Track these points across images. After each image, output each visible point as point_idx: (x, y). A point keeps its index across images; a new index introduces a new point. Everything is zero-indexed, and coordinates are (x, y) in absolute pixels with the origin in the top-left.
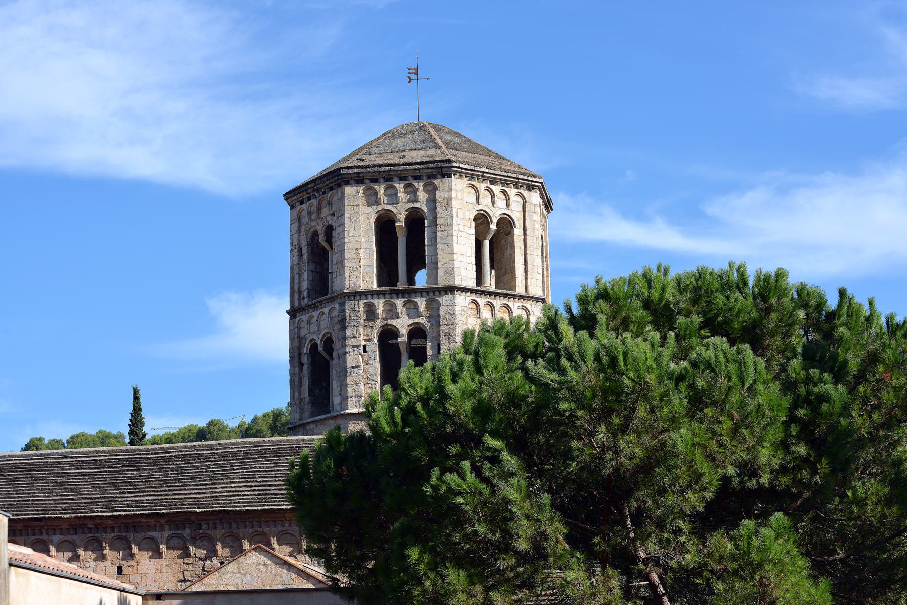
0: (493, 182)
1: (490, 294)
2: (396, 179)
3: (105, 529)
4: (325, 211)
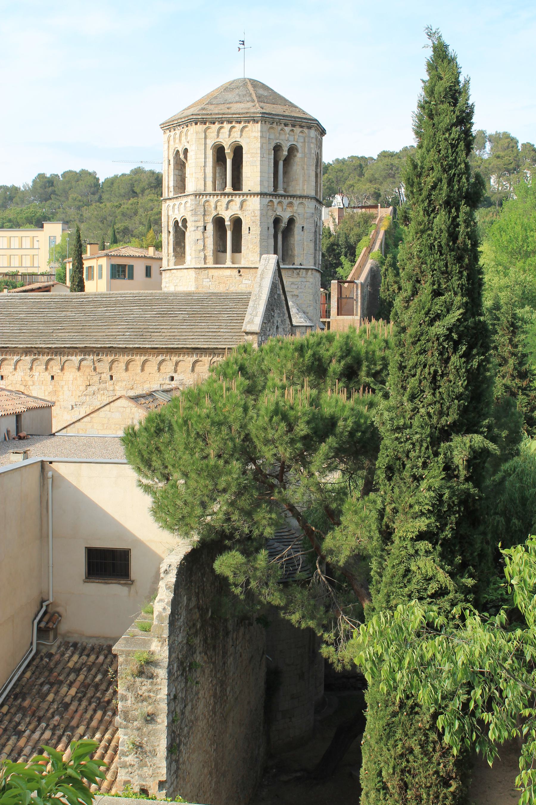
0: (286, 125)
1: (282, 196)
4: (183, 138)
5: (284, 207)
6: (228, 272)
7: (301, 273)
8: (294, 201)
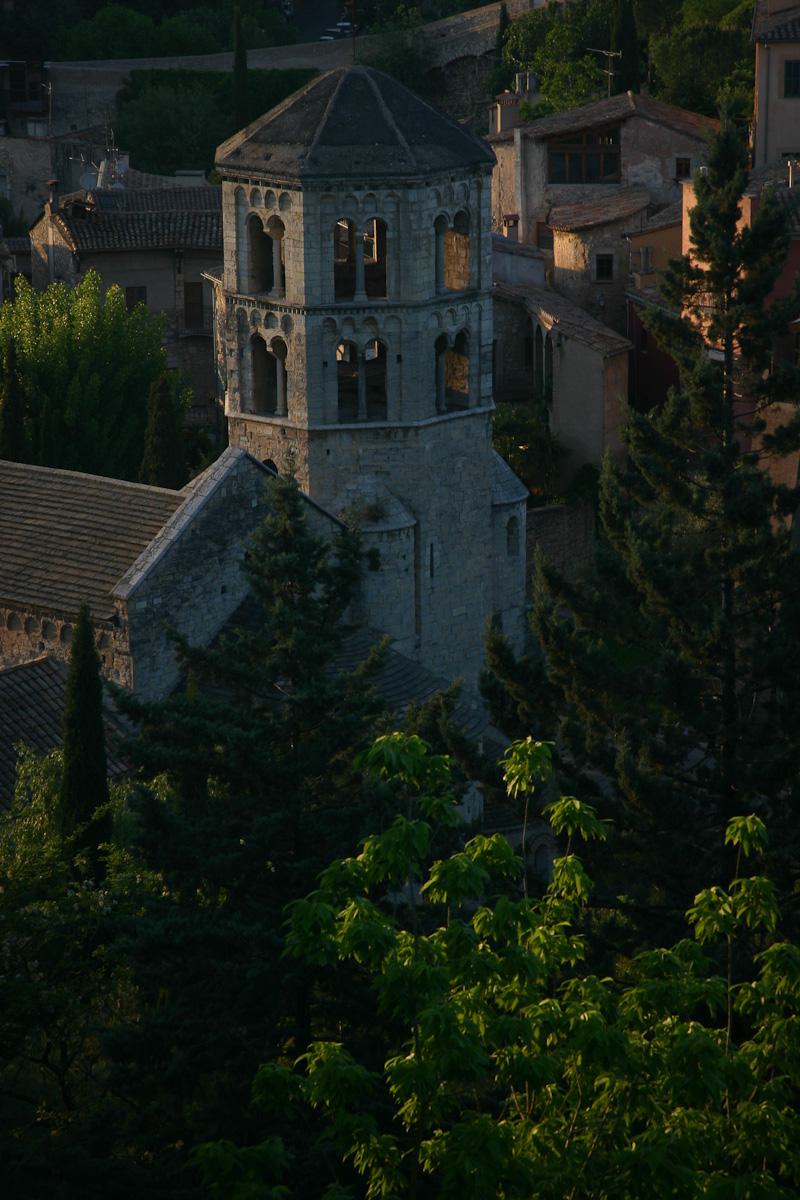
0: (358, 188)
5: (357, 327)
6: (269, 431)
7: (393, 435)
8: (376, 316)
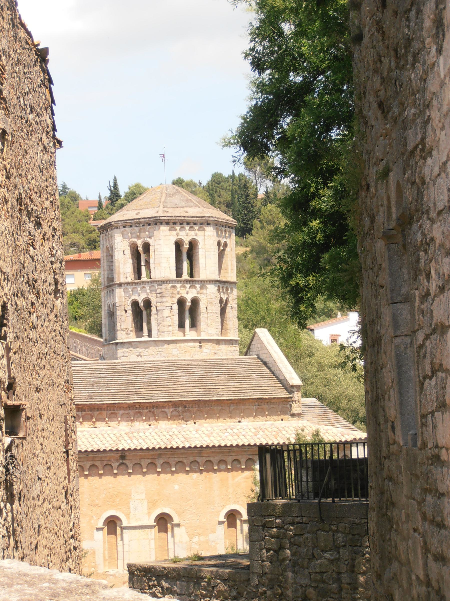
2: (185, 223)
3: (143, 408)
6: (192, 344)
